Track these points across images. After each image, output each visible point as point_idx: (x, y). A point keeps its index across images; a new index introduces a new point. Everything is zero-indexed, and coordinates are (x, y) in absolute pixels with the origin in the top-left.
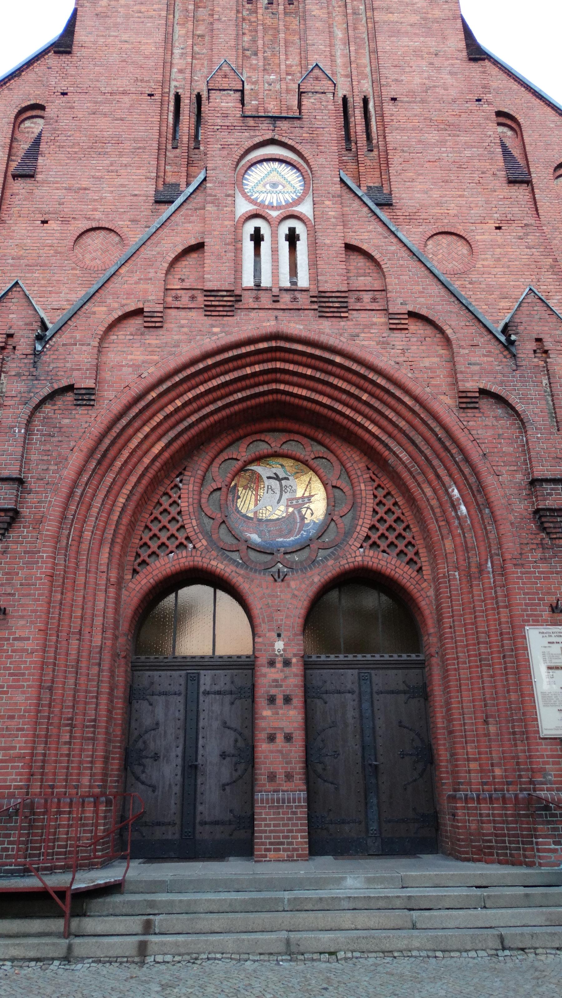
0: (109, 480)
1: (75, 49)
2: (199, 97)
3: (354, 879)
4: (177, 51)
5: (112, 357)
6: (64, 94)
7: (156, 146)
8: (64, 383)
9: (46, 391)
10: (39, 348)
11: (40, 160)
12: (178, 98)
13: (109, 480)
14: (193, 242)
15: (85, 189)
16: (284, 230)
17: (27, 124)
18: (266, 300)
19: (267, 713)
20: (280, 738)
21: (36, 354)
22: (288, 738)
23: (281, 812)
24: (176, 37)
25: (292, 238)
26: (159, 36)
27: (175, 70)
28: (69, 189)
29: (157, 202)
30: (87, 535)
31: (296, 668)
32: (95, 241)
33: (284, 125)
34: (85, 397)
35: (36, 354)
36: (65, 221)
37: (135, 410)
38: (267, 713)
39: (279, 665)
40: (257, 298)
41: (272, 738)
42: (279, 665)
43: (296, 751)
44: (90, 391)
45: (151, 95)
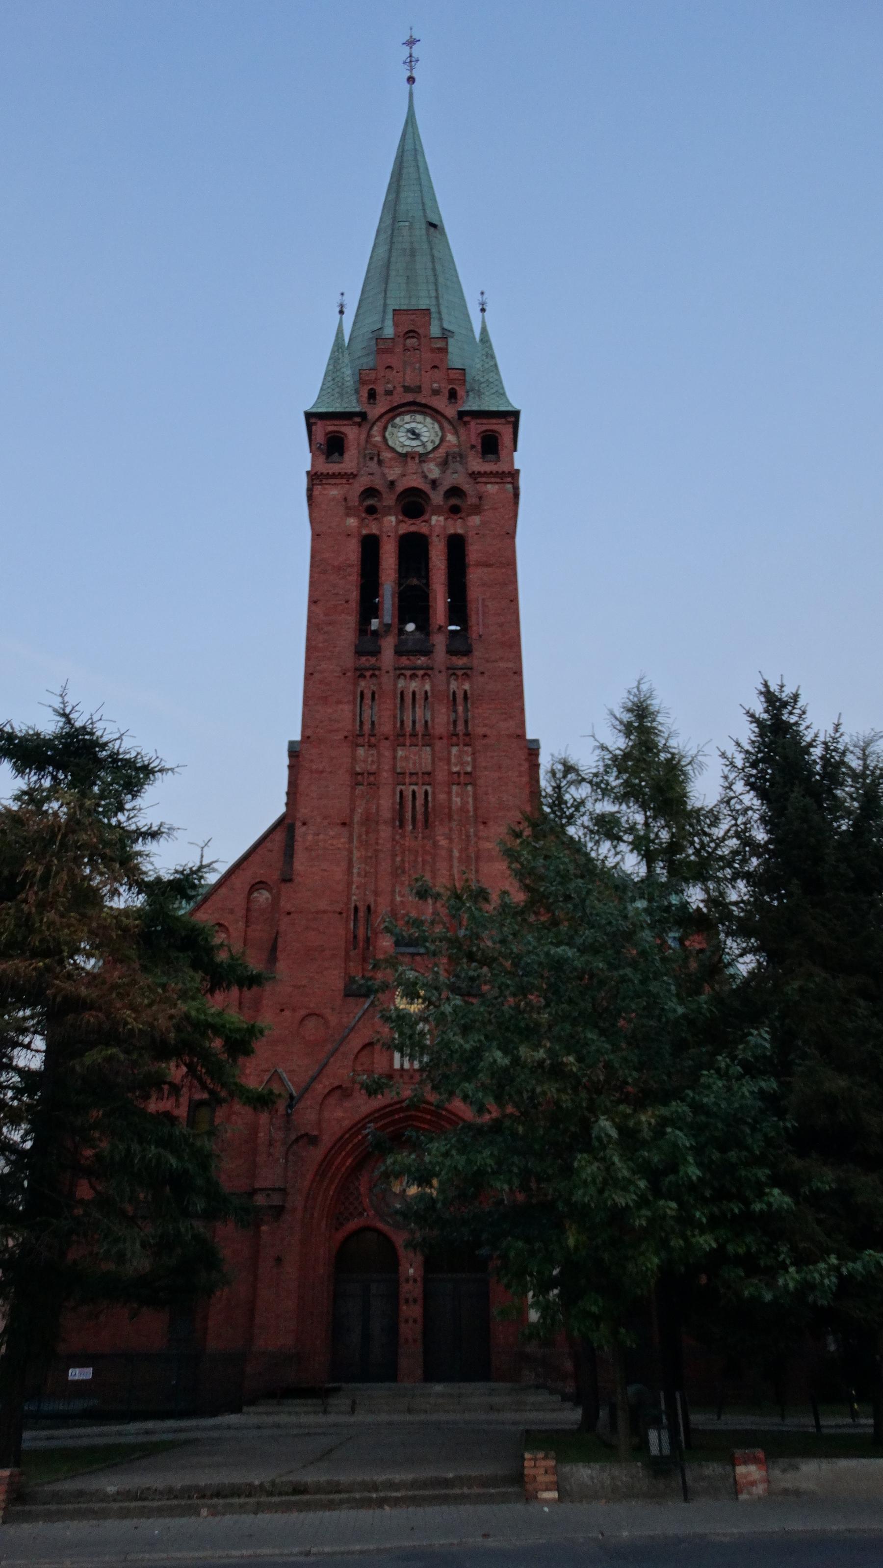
0: (325, 1184)
1: (294, 877)
2: (369, 907)
3: (438, 1388)
4: (355, 871)
5: (326, 1114)
6: (289, 913)
7: (343, 953)
8: (303, 1132)
9: (293, 1137)
10: (289, 1111)
11: (277, 964)
12: (356, 909)
13: (325, 1184)
14: (367, 1041)
15: (304, 986)
17: (255, 894)
18: (406, 1078)
19: (405, 1307)
20: (411, 1321)
21: (288, 1115)
22: (415, 1321)
23: (410, 1359)
24: (355, 859)
26: (344, 865)
27: (354, 886)
28: (294, 986)
29: (347, 995)
30: (316, 1215)
31: (419, 1284)
32: (311, 1023)
33: (418, 958)
34: (313, 1140)
35: (288, 1115)
36: (294, 1010)
37: (338, 1145)
38: (405, 1307)
39: (411, 1282)
40: (402, 1076)
41: (407, 1321)
42: (411, 1282)
43: (419, 1328)
44: (316, 1137)
45: (340, 913)
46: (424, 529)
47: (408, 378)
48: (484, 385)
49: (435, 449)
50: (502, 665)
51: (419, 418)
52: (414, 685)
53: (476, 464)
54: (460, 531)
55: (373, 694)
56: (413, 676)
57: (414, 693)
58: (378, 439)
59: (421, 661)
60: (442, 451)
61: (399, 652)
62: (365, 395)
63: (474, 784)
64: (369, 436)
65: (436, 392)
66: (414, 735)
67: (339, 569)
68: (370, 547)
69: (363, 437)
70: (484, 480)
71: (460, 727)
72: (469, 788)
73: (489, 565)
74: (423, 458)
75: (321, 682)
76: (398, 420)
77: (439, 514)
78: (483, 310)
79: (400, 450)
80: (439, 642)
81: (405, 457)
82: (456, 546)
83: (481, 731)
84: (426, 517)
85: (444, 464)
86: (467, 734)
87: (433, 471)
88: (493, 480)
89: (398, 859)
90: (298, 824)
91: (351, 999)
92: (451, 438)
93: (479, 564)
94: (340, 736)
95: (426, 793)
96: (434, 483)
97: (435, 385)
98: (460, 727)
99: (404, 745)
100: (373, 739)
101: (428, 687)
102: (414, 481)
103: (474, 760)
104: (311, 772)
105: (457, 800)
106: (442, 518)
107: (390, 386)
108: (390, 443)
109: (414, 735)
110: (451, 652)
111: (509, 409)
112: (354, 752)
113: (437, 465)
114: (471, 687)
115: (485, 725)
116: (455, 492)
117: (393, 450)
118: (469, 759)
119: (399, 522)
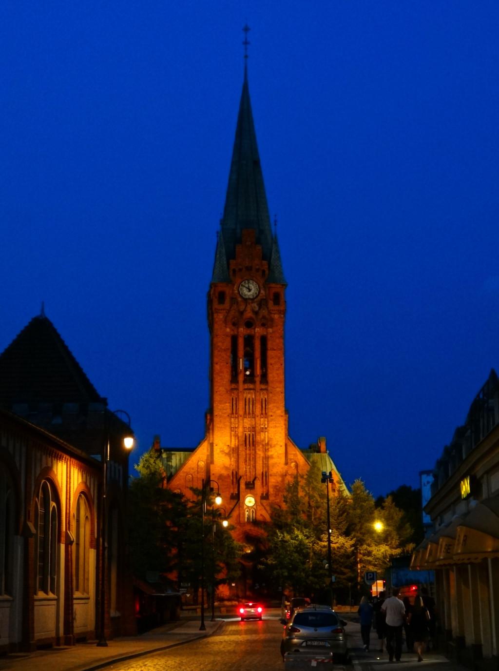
12: (233, 473)
16: (251, 511)
25: (253, 511)
46: (253, 333)
48: (275, 267)
49: (257, 297)
50: (278, 389)
52: (249, 396)
54: (265, 333)
55: (236, 399)
57: (249, 399)
58: (236, 292)
59: (251, 386)
60: (259, 298)
61: (245, 382)
63: (268, 433)
64: (233, 290)
65: (257, 270)
66: (249, 413)
67: (225, 350)
68: (234, 339)
69: (231, 292)
70: (273, 312)
71: (264, 412)
72: (266, 433)
73: (275, 350)
75: (220, 395)
76: (243, 283)
77: (258, 328)
78: (275, 225)
79: (244, 296)
80: (258, 379)
81: (246, 300)
82: (264, 340)
83: (270, 414)
84: (253, 327)
85: (260, 305)
86: (266, 414)
87: (257, 309)
89: (244, 457)
90: (214, 445)
91: (232, 501)
92: (262, 292)
93: (271, 349)
94: (227, 415)
95: (253, 434)
96: (256, 313)
97: (257, 267)
98: (264, 412)
99: (246, 418)
100: (236, 416)
101: (254, 397)
102: (249, 314)
103: (268, 424)
104: (218, 427)
105: (262, 437)
106: (259, 329)
107: (240, 267)
108: (241, 293)
109: (249, 413)
110: (261, 382)
111: (285, 284)
112: (231, 419)
113: (257, 305)
114: (268, 397)
115: (272, 412)
116: (264, 317)
117: (241, 297)
118: (266, 423)
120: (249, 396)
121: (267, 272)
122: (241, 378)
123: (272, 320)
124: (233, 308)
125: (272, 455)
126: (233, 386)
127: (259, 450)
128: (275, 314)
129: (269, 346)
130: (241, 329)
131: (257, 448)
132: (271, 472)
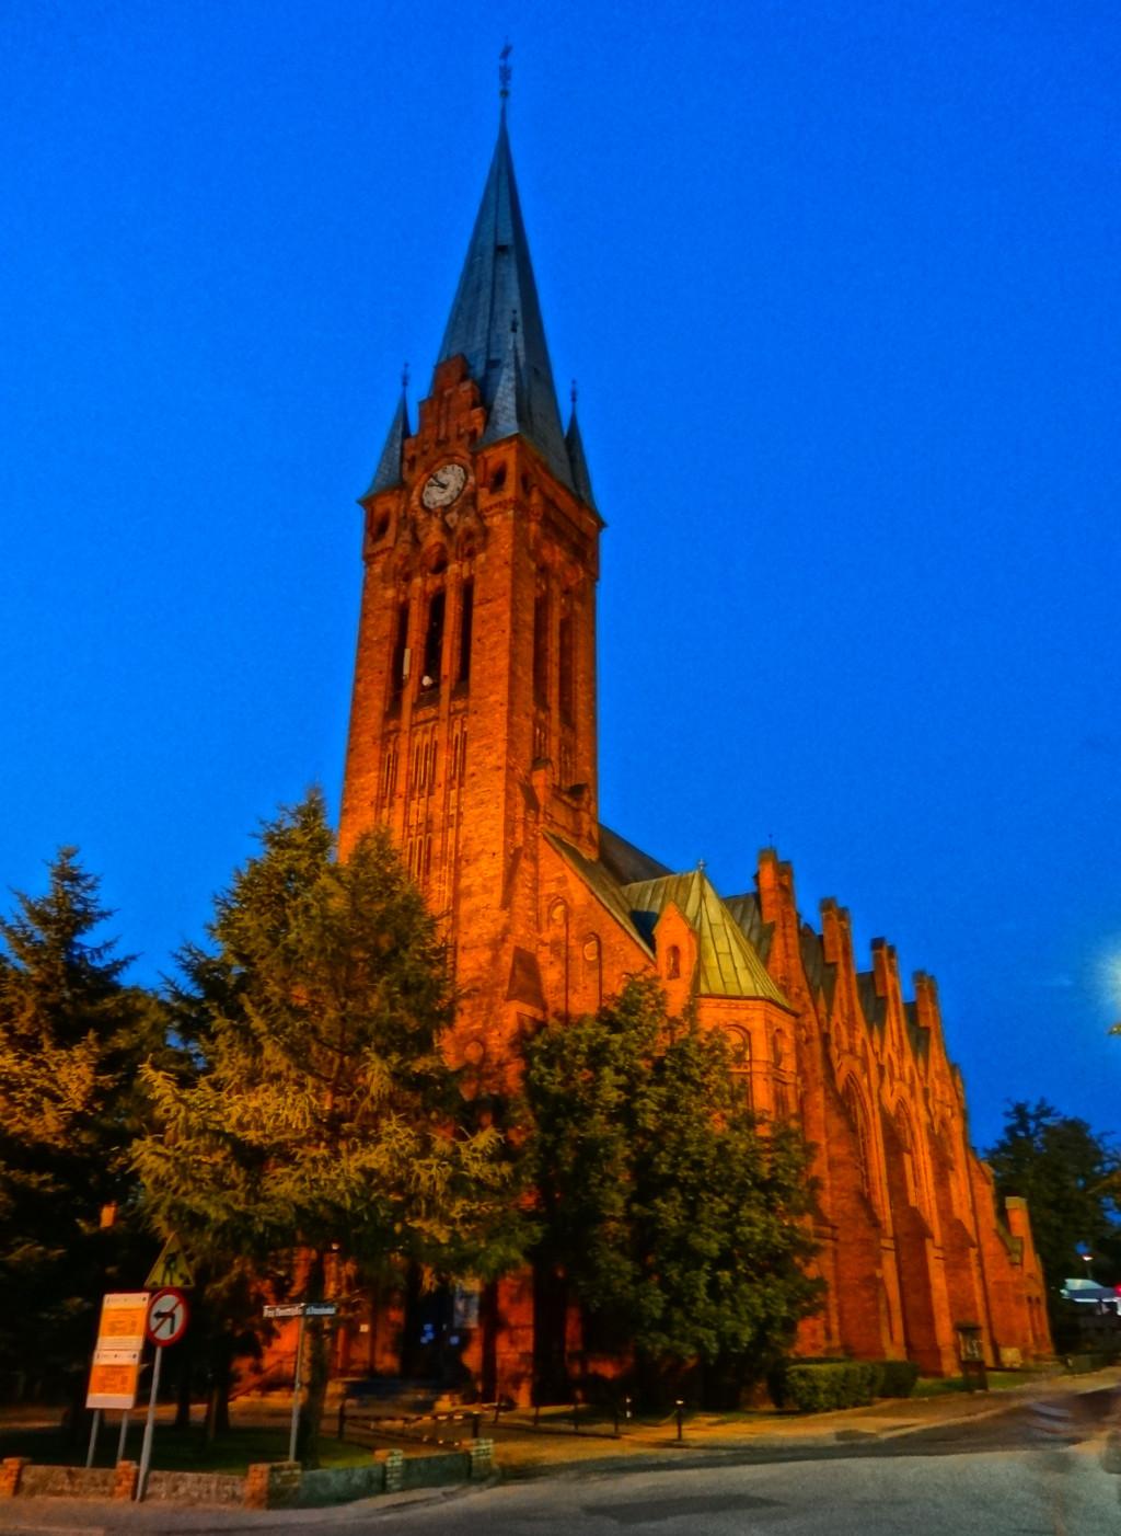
47: (443, 432)
50: (492, 699)
51: (449, 468)
52: (427, 738)
53: (485, 499)
56: (425, 732)
58: (416, 503)
59: (431, 712)
62: (406, 465)
64: (408, 502)
67: (379, 643)
68: (403, 612)
74: (446, 509)
80: (445, 689)
88: (497, 510)
107: (426, 447)
108: (426, 503)
110: (454, 695)
119: (425, 582)
120: (422, 739)
121: (480, 430)
122: (408, 698)
123: (486, 532)
124: (401, 539)
125: (469, 887)
126: (392, 725)
127: (440, 880)
128: (492, 516)
129: (477, 596)
130: (418, 581)
131: (435, 874)
132: (461, 943)
